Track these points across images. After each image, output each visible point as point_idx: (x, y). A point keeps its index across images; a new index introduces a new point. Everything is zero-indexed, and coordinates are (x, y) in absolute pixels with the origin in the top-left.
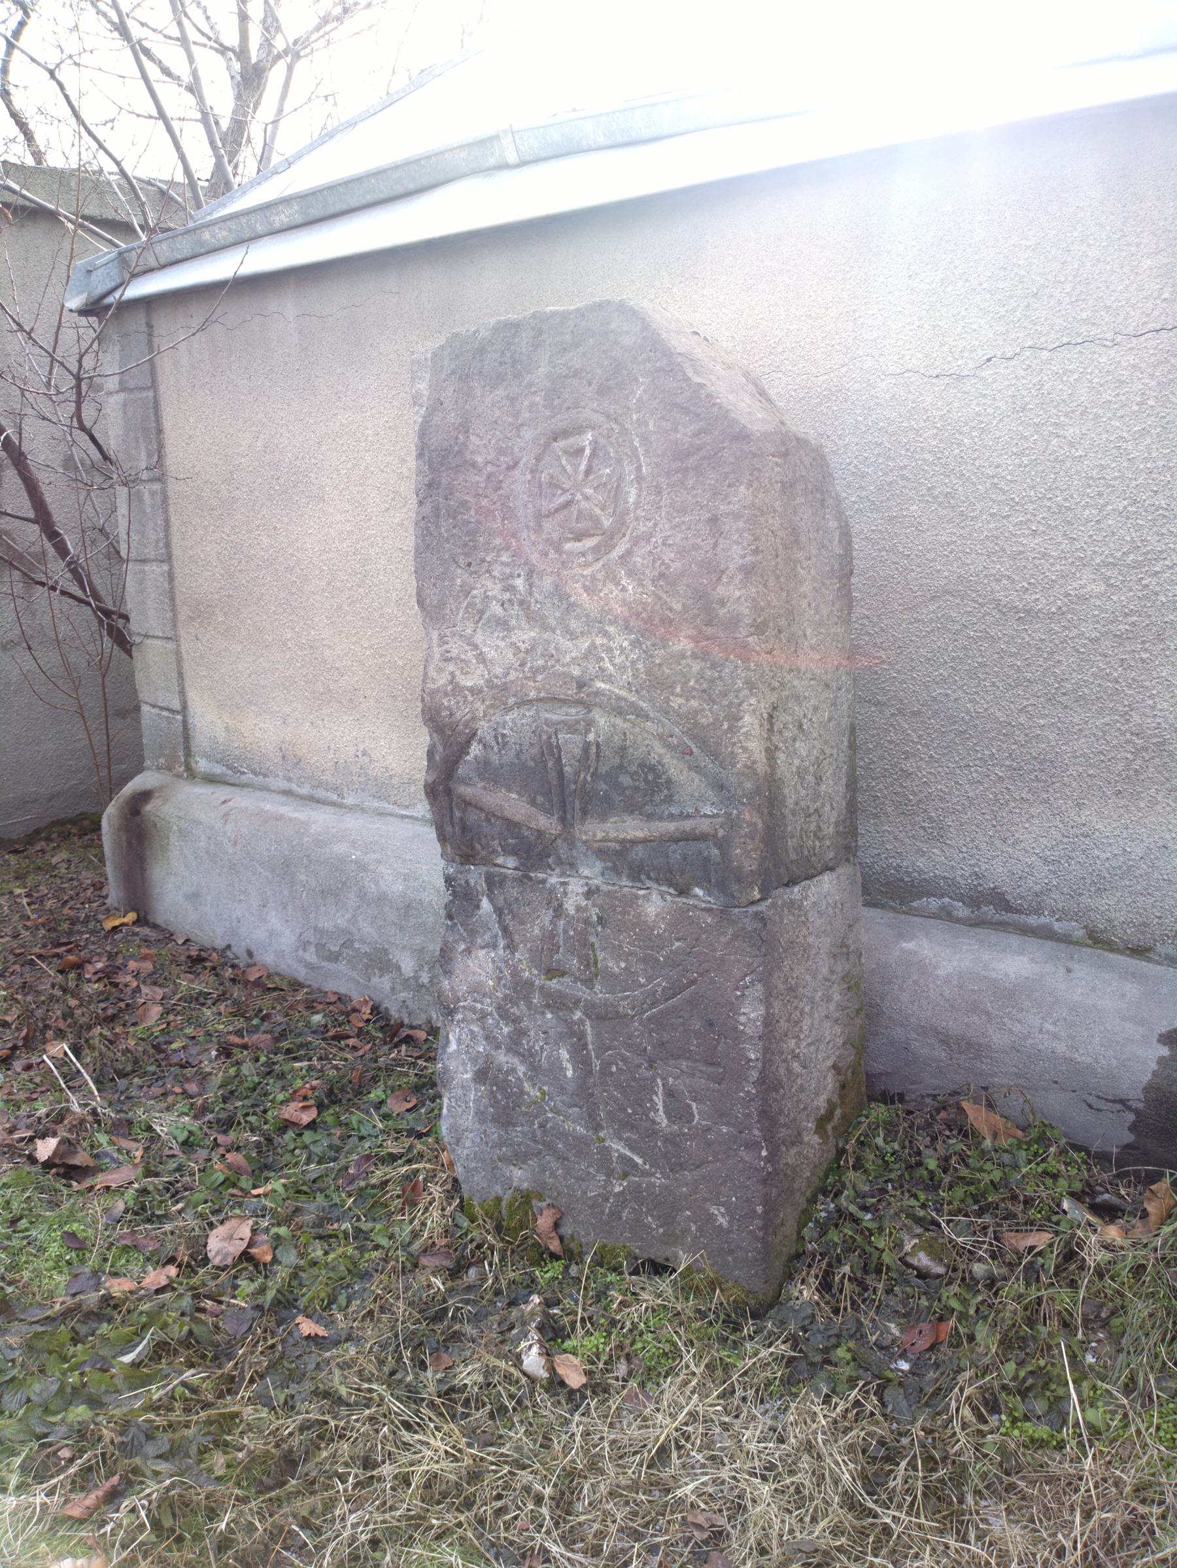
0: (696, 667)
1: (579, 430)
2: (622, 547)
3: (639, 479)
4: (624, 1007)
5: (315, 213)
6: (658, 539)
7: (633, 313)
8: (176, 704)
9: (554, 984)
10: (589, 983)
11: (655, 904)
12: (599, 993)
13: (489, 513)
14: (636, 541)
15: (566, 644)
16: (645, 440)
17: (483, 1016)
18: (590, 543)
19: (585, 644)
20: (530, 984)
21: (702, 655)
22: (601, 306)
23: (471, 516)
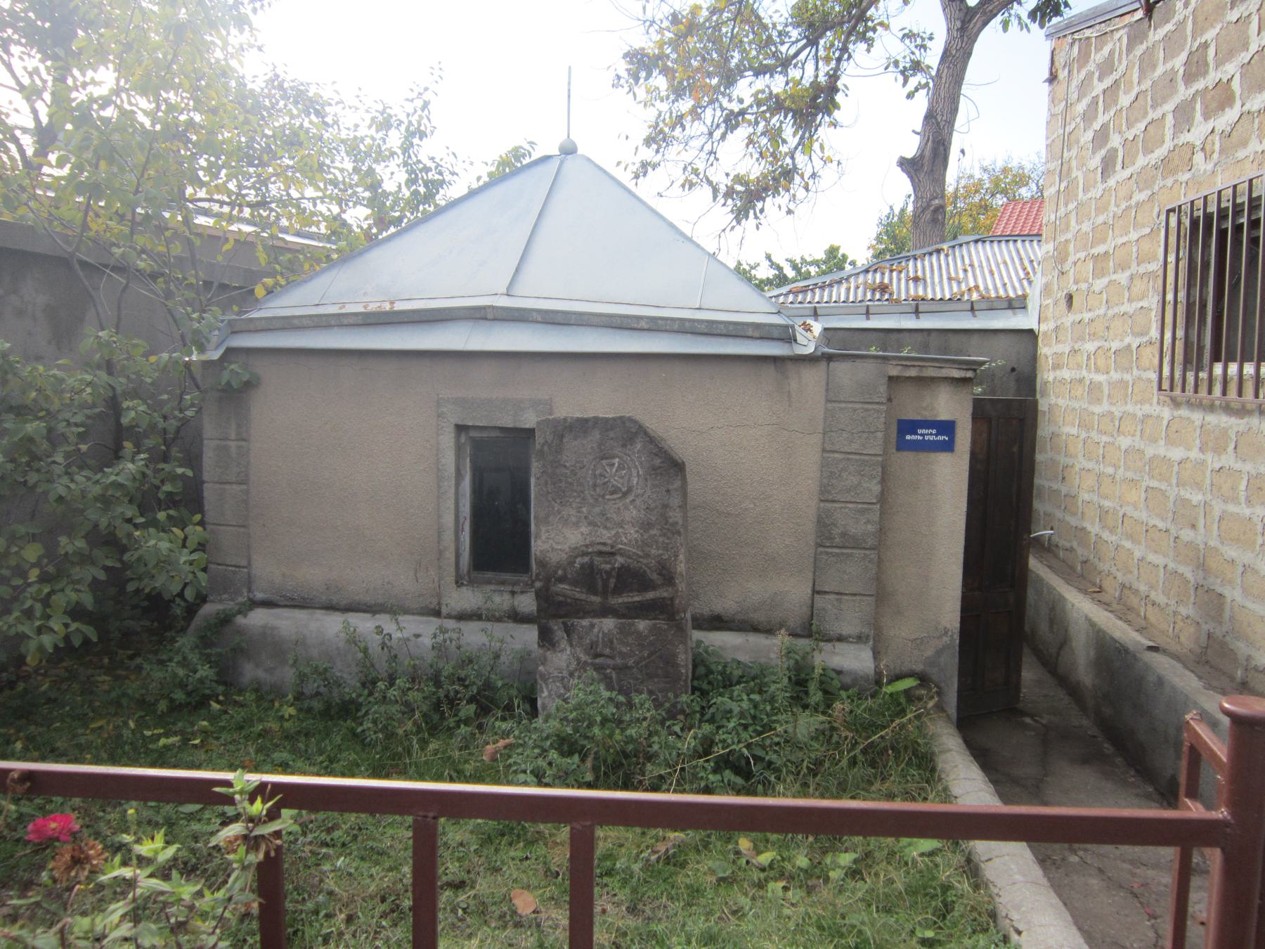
0: (661, 539)
1: (613, 457)
2: (631, 498)
3: (638, 475)
4: (631, 662)
5: (369, 321)
6: (646, 496)
7: (635, 422)
8: (244, 563)
9: (597, 661)
10: (612, 657)
11: (642, 625)
12: (619, 661)
13: (571, 484)
14: (637, 496)
15: (605, 532)
16: (641, 463)
17: (563, 678)
18: (615, 496)
19: (613, 532)
20: (585, 662)
21: (664, 535)
22: (621, 418)
23: (563, 485)
